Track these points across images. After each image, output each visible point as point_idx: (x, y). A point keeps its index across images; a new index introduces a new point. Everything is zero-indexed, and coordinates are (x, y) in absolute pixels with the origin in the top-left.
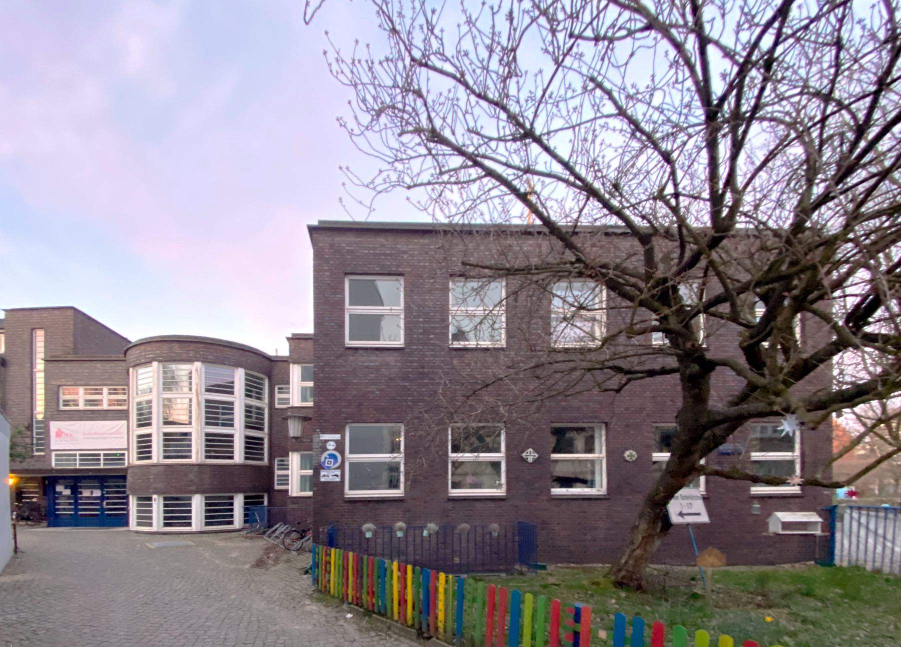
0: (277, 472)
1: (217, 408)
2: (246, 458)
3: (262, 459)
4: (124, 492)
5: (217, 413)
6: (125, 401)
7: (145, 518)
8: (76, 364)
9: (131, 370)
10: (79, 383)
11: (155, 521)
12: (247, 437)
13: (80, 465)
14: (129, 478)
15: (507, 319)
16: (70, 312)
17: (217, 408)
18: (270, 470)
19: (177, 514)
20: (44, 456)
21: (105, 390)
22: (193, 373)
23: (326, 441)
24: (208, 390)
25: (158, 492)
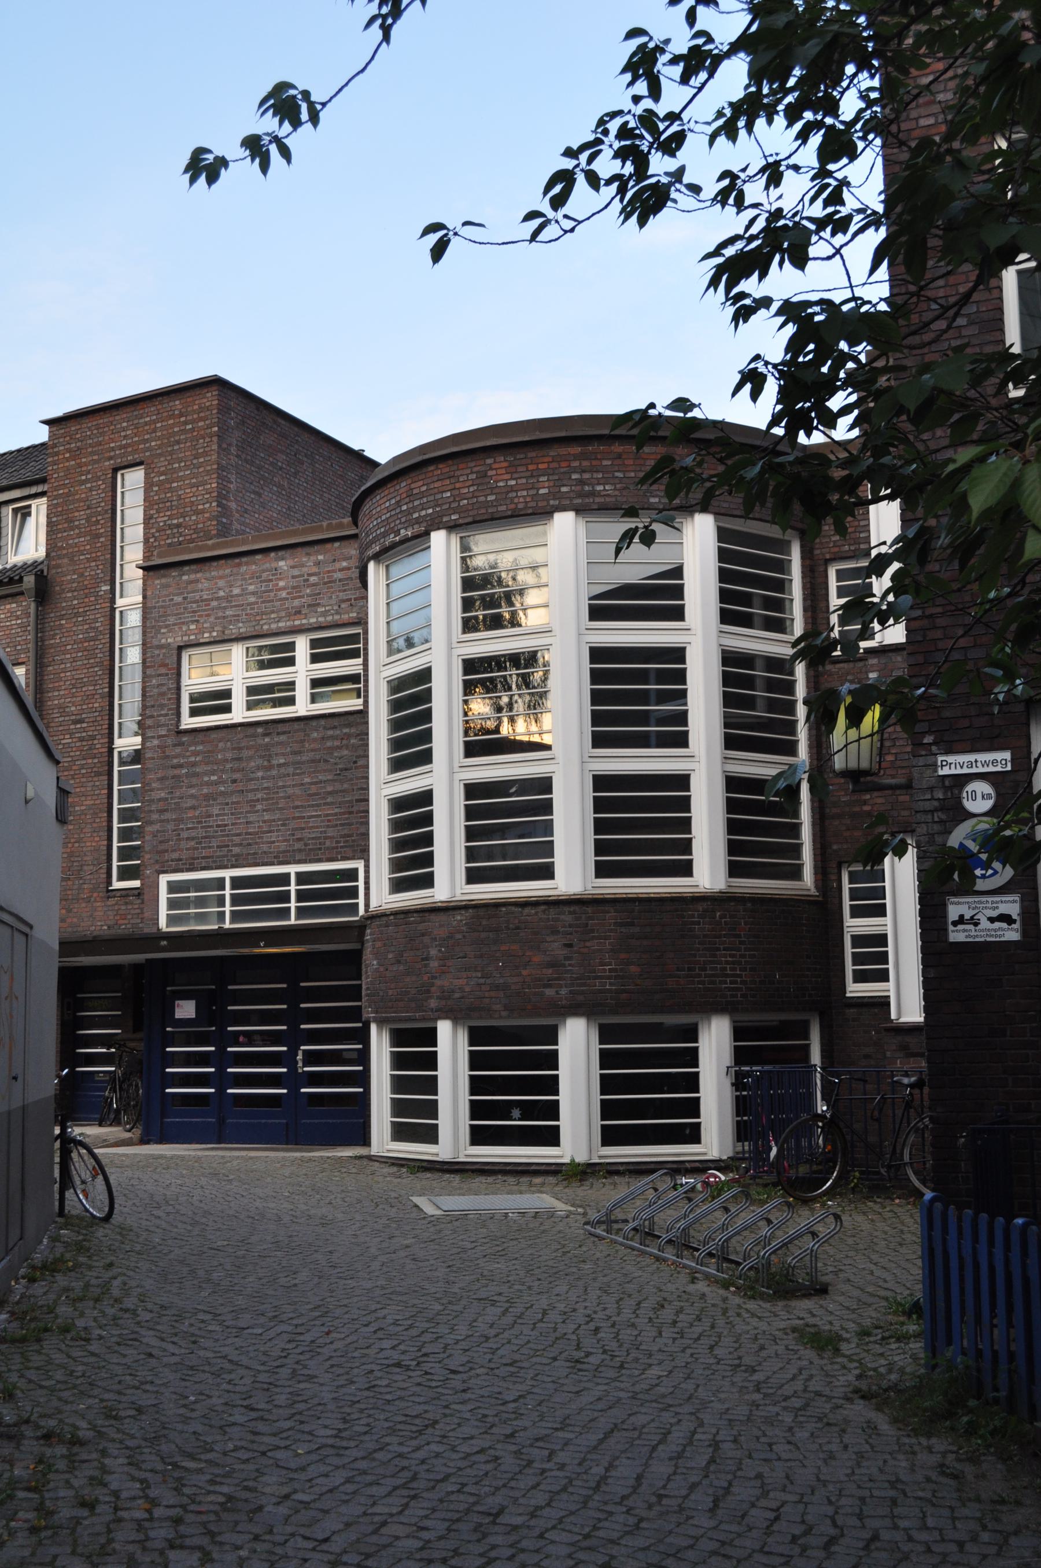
0: (854, 925)
1: (642, 676)
2: (602, 870)
3: (173, 887)
4: (355, 1014)
5: (632, 695)
6: (354, 678)
7: (416, 1118)
8: (225, 569)
9: (371, 566)
10: (233, 630)
11: (444, 1121)
12: (601, 782)
13: (236, 916)
14: (370, 962)
15: (899, 188)
16: (210, 398)
17: (642, 676)
18: (823, 911)
19: (514, 1097)
20: (138, 893)
21: (302, 647)
22: (556, 562)
23: (961, 781)
24: (597, 613)
25: (455, 1016)
